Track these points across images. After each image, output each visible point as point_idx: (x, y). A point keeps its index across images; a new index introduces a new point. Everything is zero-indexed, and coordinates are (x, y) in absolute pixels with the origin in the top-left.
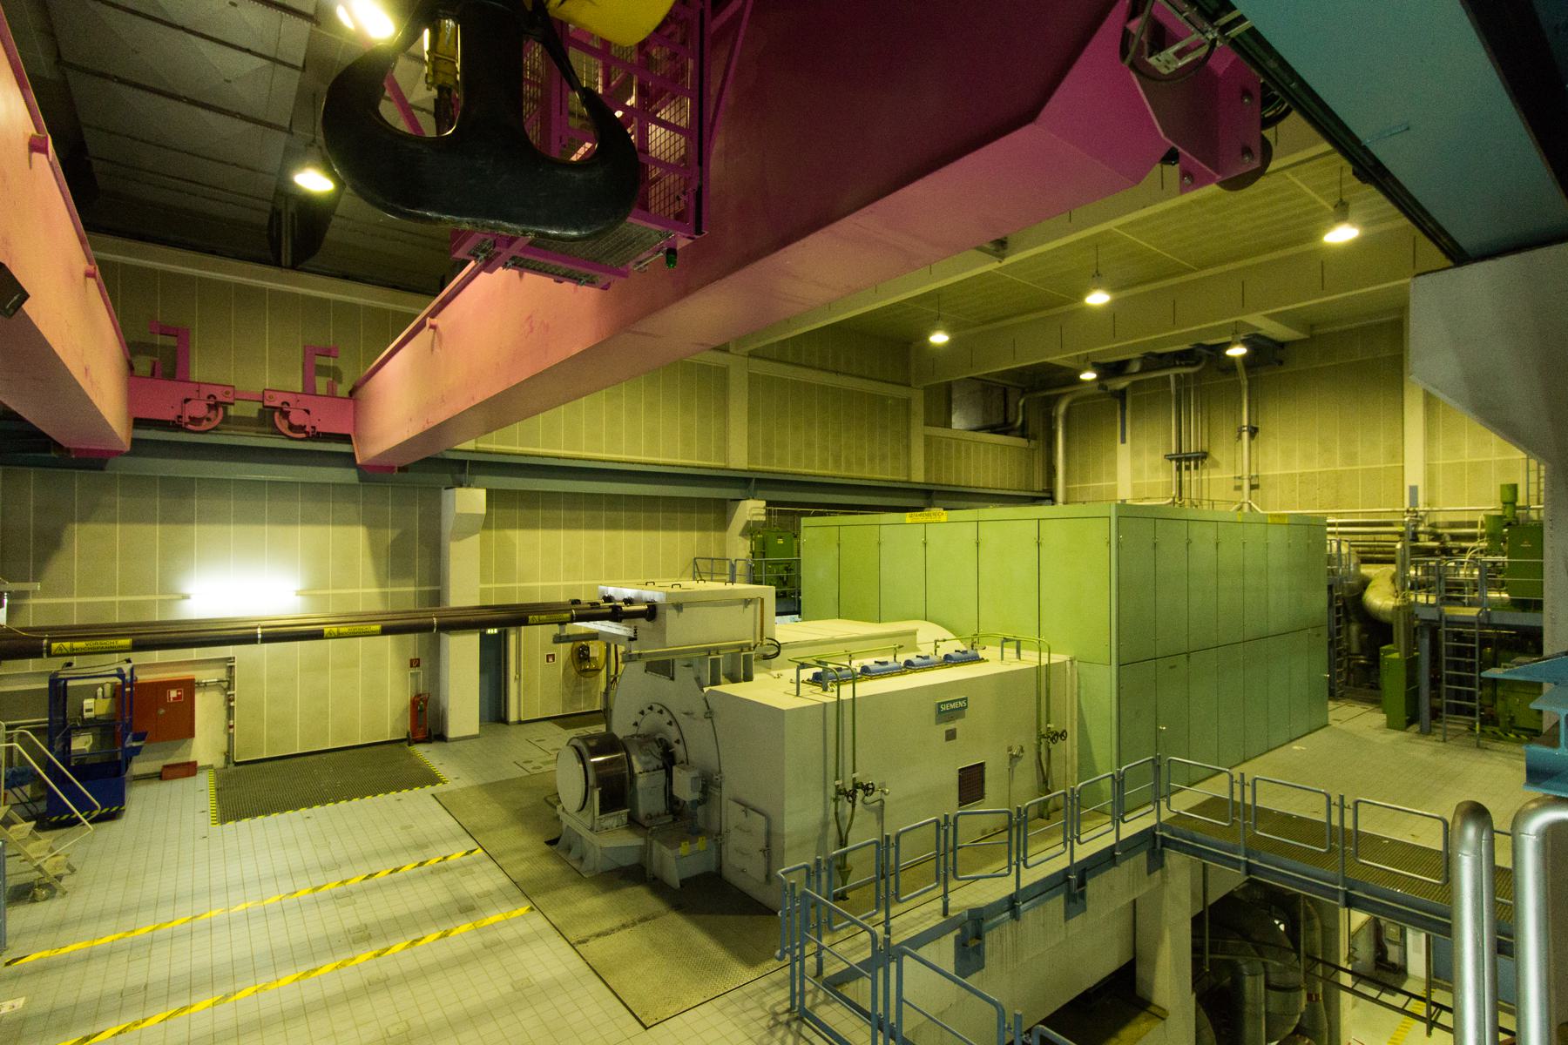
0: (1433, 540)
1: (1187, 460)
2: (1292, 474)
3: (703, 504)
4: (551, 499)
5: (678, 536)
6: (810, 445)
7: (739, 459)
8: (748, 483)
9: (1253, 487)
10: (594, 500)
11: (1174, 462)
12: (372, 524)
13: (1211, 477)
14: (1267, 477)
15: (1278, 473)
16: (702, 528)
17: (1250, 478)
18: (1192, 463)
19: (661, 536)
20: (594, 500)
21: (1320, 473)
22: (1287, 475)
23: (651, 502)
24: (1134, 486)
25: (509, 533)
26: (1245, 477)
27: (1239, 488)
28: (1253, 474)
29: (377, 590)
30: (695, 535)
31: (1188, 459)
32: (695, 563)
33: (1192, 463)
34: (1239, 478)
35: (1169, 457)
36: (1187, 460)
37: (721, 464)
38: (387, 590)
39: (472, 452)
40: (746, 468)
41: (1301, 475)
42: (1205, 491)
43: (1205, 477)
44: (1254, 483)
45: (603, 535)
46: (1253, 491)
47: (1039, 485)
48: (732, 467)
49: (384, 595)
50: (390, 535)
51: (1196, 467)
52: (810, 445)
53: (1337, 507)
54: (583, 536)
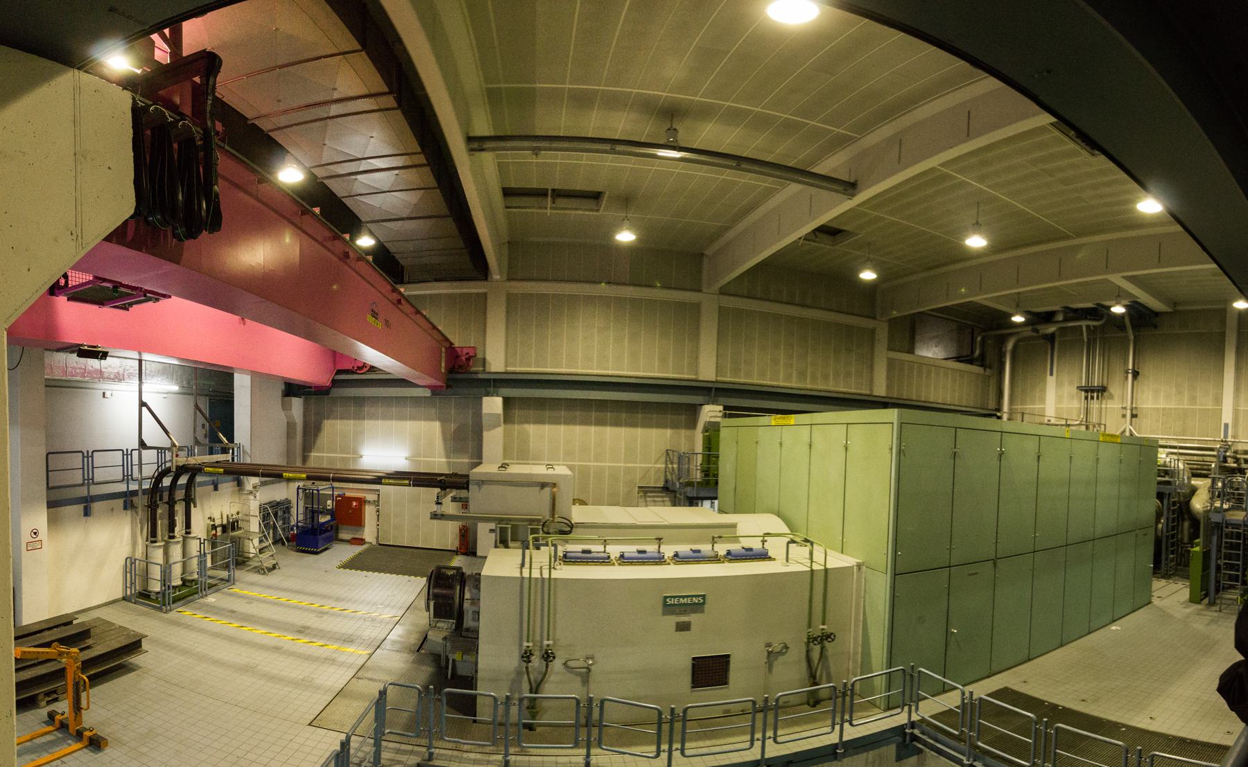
0: (1234, 463)
1: (1094, 391)
2: (1158, 408)
3: (676, 408)
4: (555, 403)
5: (654, 433)
6: (775, 362)
7: (707, 372)
8: (712, 392)
9: (1134, 416)
10: (586, 404)
11: (1083, 393)
12: (443, 420)
13: (1108, 406)
14: (1142, 408)
15: (1150, 406)
16: (674, 426)
17: (1132, 410)
18: (1089, 394)
19: (639, 431)
20: (586, 404)
21: (1175, 409)
22: (1155, 408)
23: (632, 406)
24: (1057, 409)
25: (527, 426)
26: (1129, 408)
27: (1124, 416)
28: (1134, 406)
29: (444, 460)
30: (668, 432)
31: (1093, 391)
32: (668, 454)
33: (1095, 394)
34: (1125, 408)
35: (1080, 388)
36: (1094, 391)
37: (693, 377)
38: (449, 460)
39: (504, 373)
40: (714, 380)
41: (1164, 409)
42: (1103, 418)
43: (1103, 406)
44: (1134, 413)
45: (593, 429)
46: (1134, 419)
47: (992, 405)
48: (701, 378)
49: (449, 463)
50: (453, 427)
51: (1098, 398)
52: (775, 362)
53: (1183, 435)
54: (578, 429)
